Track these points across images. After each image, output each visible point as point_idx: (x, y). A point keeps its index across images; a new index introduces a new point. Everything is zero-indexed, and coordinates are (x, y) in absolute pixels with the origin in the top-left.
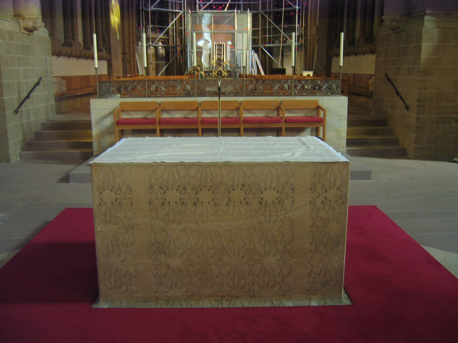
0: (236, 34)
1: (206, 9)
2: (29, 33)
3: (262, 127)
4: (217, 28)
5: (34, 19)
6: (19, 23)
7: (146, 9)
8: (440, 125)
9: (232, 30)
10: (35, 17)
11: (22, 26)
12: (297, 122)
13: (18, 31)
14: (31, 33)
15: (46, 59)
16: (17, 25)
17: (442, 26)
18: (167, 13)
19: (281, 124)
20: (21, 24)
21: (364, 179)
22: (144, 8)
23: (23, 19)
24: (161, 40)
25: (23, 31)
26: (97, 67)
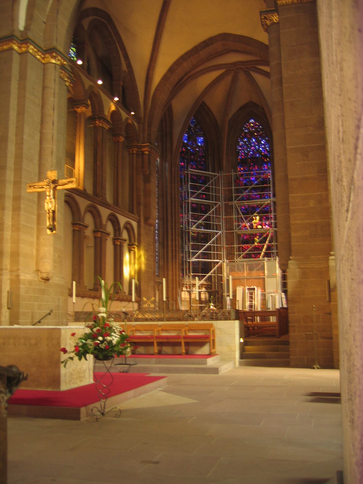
0: (266, 278)
1: (244, 257)
2: (46, 281)
3: (168, 341)
4: (249, 274)
5: (48, 272)
6: (38, 275)
7: (188, 260)
8: (309, 340)
9: (263, 276)
10: (48, 271)
11: (39, 277)
12: (195, 338)
13: (37, 280)
14: (47, 281)
15: (59, 299)
16: (37, 276)
17: (302, 267)
18: (211, 262)
19: (181, 339)
20: (39, 275)
21: (213, 374)
22: (187, 259)
23: (41, 272)
24: (204, 286)
25: (40, 280)
26: (74, 302)
